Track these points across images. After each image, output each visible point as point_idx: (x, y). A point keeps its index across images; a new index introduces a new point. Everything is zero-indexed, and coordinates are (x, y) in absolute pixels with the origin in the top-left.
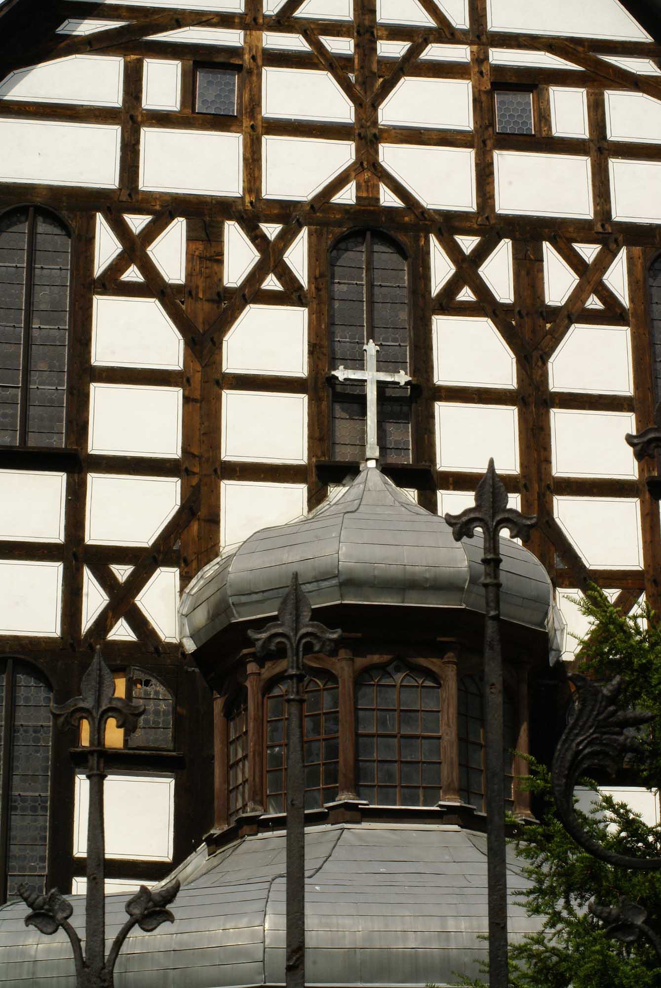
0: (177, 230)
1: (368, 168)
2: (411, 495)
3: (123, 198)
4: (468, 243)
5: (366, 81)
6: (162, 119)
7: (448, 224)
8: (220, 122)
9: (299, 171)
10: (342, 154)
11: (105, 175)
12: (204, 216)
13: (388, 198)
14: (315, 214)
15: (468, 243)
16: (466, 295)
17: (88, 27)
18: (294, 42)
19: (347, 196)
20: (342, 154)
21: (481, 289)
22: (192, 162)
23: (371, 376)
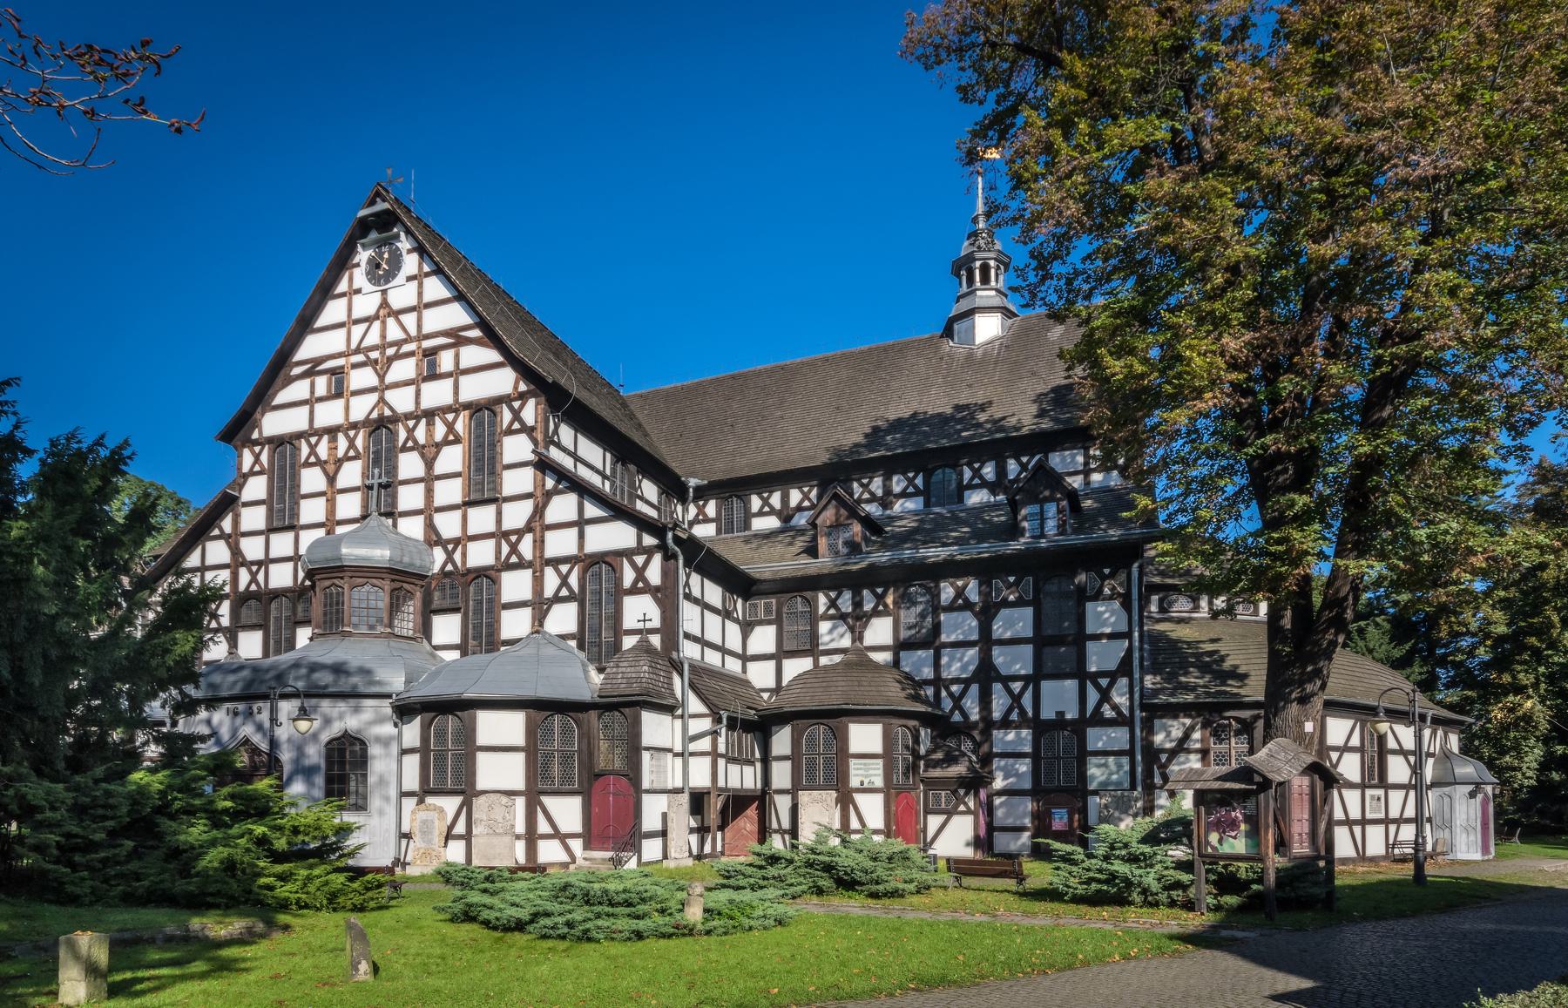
0: (326, 438)
1: (382, 400)
4: (411, 423)
5: (381, 367)
6: (320, 400)
7: (408, 416)
8: (338, 394)
9: (361, 408)
10: (374, 397)
12: (332, 431)
13: (387, 412)
14: (366, 422)
16: (410, 444)
17: (297, 371)
18: (360, 358)
19: (375, 415)
20: (374, 397)
21: (415, 441)
23: (376, 482)
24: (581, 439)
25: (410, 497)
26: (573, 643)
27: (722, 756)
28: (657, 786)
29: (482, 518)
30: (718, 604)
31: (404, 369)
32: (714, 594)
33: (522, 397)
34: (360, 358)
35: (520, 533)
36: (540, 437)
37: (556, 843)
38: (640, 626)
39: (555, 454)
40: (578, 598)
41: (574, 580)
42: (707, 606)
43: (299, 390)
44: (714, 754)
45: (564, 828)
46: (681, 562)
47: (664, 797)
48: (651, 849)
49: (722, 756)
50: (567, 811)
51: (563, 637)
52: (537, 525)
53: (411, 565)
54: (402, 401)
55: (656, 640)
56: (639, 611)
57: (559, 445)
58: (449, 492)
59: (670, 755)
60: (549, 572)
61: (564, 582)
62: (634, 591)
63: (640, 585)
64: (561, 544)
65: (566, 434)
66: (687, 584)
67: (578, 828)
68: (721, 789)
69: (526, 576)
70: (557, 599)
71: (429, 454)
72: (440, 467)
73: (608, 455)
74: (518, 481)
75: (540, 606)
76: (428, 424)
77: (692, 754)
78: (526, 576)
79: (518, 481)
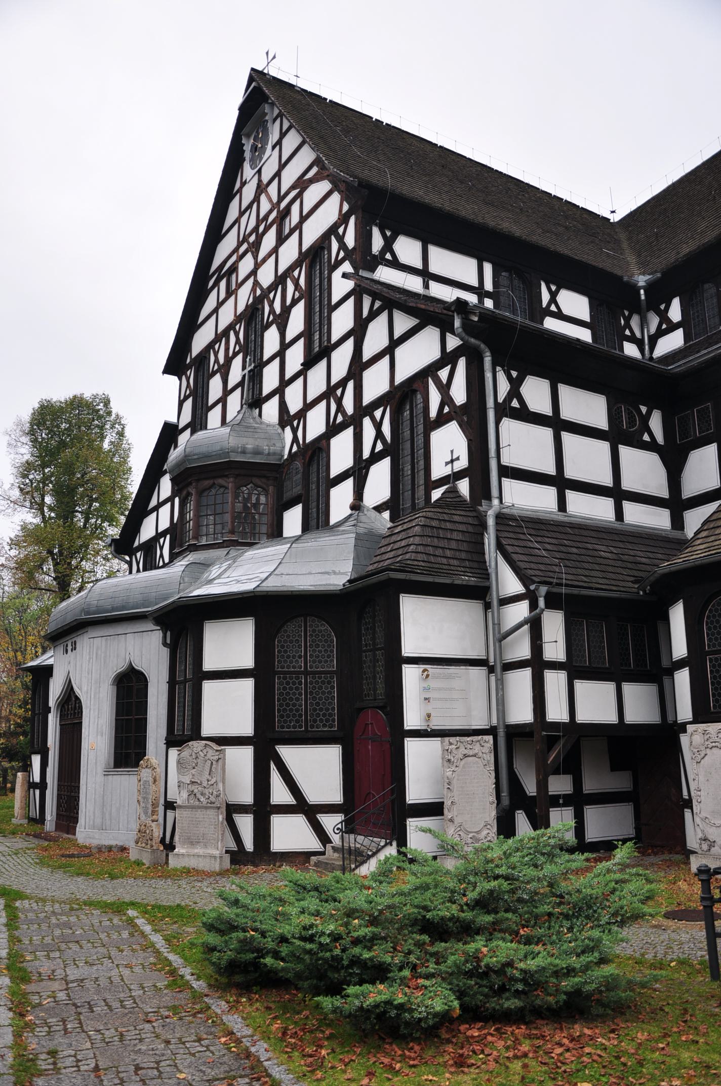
1: (256, 283)
2: (257, 410)
3: (218, 339)
9: (244, 296)
11: (212, 336)
15: (271, 296)
22: (227, 316)
24: (434, 252)
25: (270, 379)
26: (386, 515)
27: (555, 666)
28: (437, 723)
29: (317, 380)
30: (601, 421)
31: (269, 241)
32: (587, 407)
33: (343, 219)
34: (245, 247)
35: (343, 383)
36: (357, 256)
37: (299, 821)
38: (447, 471)
39: (385, 274)
40: (392, 450)
41: (386, 429)
42: (558, 425)
43: (211, 303)
44: (538, 664)
45: (313, 797)
46: (488, 360)
47: (435, 744)
48: (419, 835)
49: (555, 666)
50: (318, 769)
51: (379, 509)
52: (358, 367)
53: (257, 452)
54: (266, 276)
55: (464, 486)
56: (448, 447)
57: (396, 264)
58: (295, 357)
59: (478, 673)
60: (367, 423)
61: (379, 435)
62: (442, 420)
63: (446, 409)
64: (376, 383)
65: (408, 249)
66: (515, 392)
67: (336, 796)
68: (556, 725)
69: (348, 434)
70: (375, 457)
71: (282, 321)
72: (289, 337)
73: (488, 268)
74: (342, 321)
75: (359, 473)
76: (282, 288)
77: (510, 666)
78: (348, 434)
79: (342, 321)
